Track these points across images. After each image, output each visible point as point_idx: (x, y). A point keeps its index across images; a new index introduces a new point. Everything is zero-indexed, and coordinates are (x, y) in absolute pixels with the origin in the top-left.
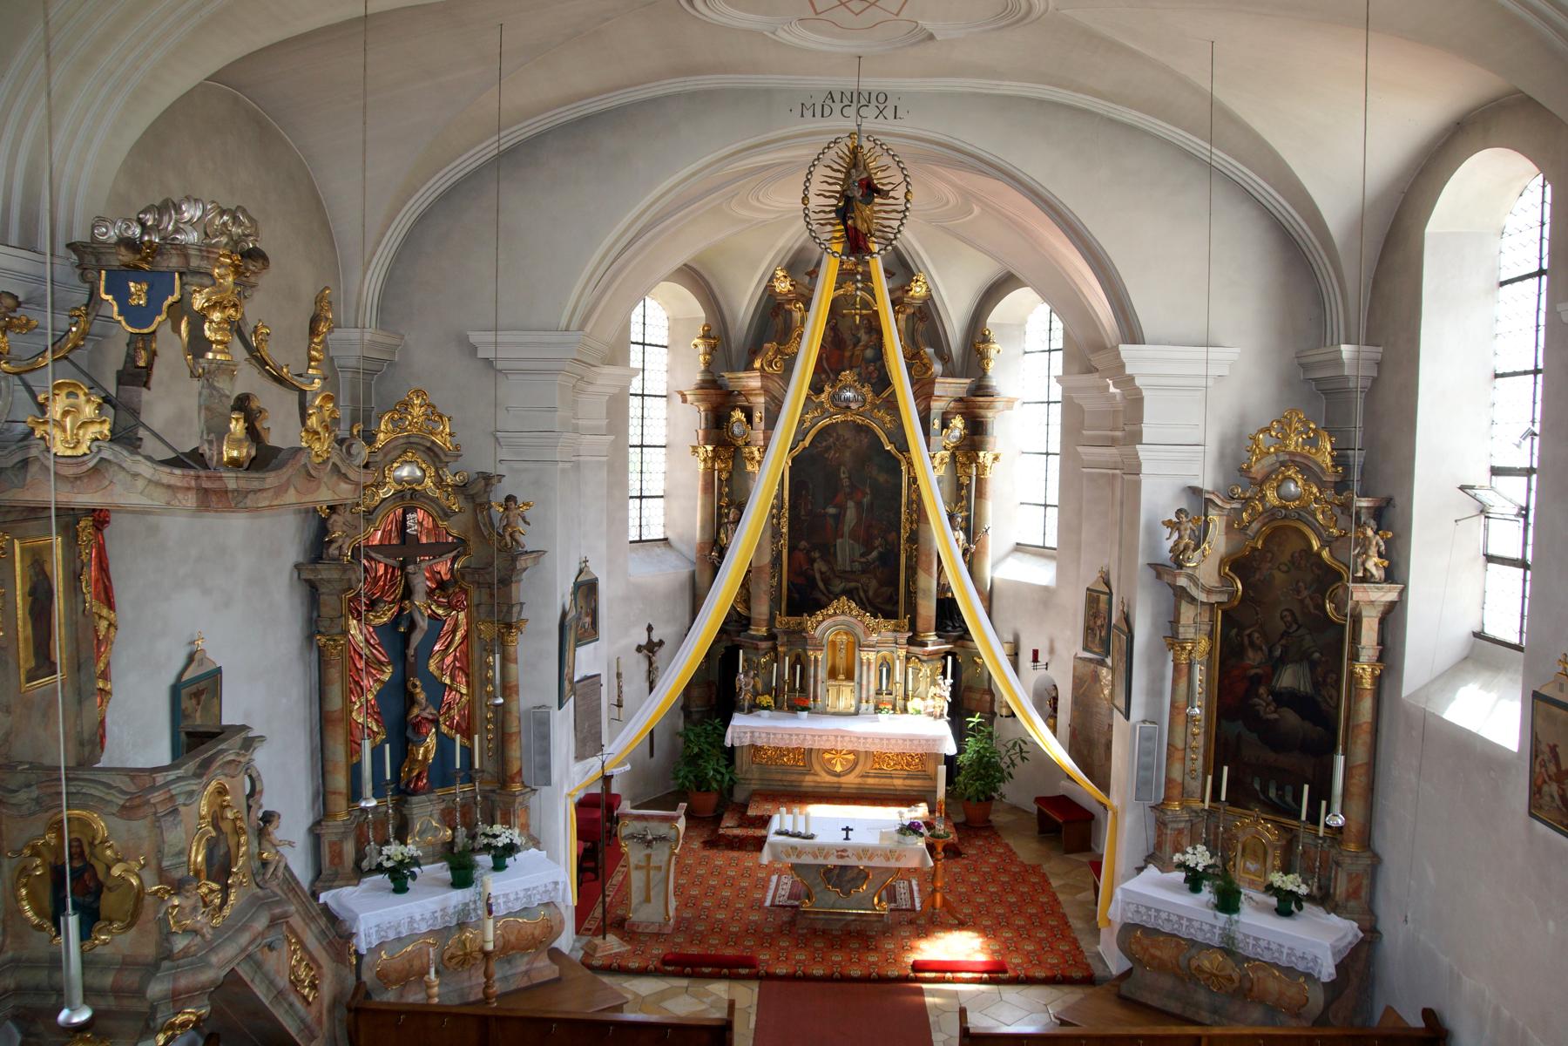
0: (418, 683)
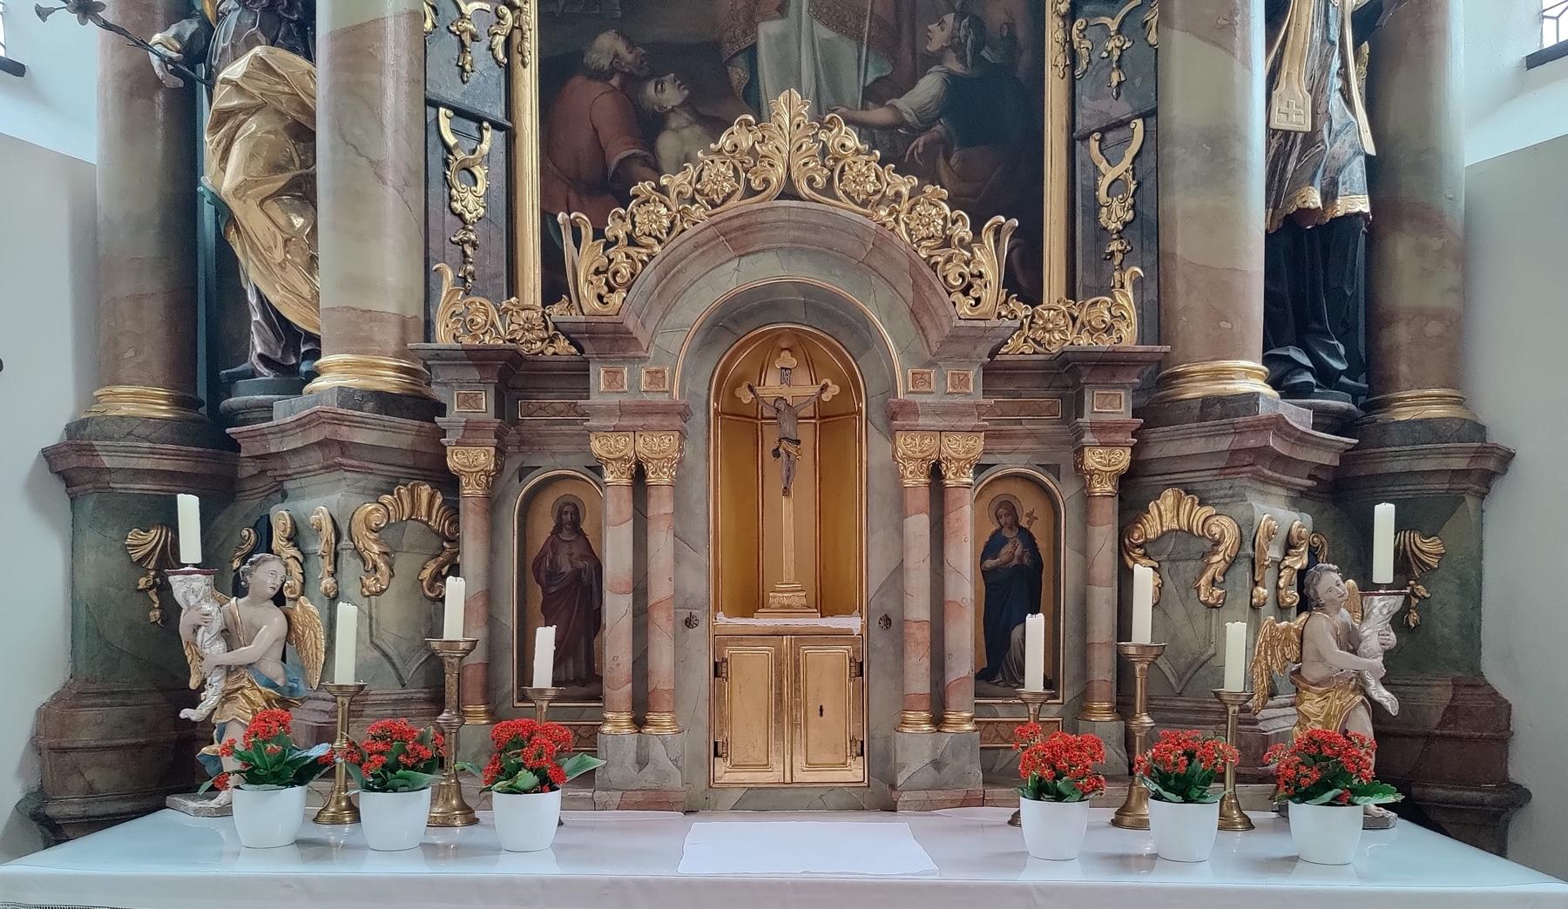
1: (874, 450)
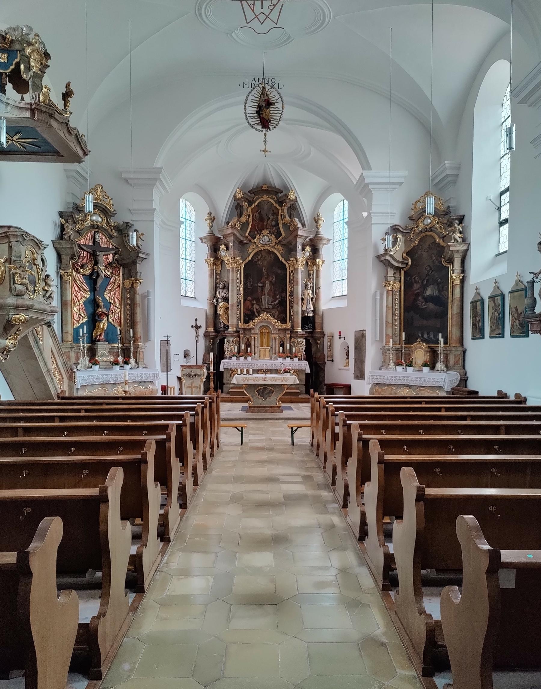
0: (100, 298)
1: (270, 335)
